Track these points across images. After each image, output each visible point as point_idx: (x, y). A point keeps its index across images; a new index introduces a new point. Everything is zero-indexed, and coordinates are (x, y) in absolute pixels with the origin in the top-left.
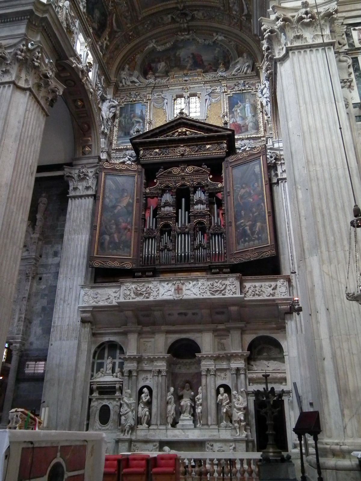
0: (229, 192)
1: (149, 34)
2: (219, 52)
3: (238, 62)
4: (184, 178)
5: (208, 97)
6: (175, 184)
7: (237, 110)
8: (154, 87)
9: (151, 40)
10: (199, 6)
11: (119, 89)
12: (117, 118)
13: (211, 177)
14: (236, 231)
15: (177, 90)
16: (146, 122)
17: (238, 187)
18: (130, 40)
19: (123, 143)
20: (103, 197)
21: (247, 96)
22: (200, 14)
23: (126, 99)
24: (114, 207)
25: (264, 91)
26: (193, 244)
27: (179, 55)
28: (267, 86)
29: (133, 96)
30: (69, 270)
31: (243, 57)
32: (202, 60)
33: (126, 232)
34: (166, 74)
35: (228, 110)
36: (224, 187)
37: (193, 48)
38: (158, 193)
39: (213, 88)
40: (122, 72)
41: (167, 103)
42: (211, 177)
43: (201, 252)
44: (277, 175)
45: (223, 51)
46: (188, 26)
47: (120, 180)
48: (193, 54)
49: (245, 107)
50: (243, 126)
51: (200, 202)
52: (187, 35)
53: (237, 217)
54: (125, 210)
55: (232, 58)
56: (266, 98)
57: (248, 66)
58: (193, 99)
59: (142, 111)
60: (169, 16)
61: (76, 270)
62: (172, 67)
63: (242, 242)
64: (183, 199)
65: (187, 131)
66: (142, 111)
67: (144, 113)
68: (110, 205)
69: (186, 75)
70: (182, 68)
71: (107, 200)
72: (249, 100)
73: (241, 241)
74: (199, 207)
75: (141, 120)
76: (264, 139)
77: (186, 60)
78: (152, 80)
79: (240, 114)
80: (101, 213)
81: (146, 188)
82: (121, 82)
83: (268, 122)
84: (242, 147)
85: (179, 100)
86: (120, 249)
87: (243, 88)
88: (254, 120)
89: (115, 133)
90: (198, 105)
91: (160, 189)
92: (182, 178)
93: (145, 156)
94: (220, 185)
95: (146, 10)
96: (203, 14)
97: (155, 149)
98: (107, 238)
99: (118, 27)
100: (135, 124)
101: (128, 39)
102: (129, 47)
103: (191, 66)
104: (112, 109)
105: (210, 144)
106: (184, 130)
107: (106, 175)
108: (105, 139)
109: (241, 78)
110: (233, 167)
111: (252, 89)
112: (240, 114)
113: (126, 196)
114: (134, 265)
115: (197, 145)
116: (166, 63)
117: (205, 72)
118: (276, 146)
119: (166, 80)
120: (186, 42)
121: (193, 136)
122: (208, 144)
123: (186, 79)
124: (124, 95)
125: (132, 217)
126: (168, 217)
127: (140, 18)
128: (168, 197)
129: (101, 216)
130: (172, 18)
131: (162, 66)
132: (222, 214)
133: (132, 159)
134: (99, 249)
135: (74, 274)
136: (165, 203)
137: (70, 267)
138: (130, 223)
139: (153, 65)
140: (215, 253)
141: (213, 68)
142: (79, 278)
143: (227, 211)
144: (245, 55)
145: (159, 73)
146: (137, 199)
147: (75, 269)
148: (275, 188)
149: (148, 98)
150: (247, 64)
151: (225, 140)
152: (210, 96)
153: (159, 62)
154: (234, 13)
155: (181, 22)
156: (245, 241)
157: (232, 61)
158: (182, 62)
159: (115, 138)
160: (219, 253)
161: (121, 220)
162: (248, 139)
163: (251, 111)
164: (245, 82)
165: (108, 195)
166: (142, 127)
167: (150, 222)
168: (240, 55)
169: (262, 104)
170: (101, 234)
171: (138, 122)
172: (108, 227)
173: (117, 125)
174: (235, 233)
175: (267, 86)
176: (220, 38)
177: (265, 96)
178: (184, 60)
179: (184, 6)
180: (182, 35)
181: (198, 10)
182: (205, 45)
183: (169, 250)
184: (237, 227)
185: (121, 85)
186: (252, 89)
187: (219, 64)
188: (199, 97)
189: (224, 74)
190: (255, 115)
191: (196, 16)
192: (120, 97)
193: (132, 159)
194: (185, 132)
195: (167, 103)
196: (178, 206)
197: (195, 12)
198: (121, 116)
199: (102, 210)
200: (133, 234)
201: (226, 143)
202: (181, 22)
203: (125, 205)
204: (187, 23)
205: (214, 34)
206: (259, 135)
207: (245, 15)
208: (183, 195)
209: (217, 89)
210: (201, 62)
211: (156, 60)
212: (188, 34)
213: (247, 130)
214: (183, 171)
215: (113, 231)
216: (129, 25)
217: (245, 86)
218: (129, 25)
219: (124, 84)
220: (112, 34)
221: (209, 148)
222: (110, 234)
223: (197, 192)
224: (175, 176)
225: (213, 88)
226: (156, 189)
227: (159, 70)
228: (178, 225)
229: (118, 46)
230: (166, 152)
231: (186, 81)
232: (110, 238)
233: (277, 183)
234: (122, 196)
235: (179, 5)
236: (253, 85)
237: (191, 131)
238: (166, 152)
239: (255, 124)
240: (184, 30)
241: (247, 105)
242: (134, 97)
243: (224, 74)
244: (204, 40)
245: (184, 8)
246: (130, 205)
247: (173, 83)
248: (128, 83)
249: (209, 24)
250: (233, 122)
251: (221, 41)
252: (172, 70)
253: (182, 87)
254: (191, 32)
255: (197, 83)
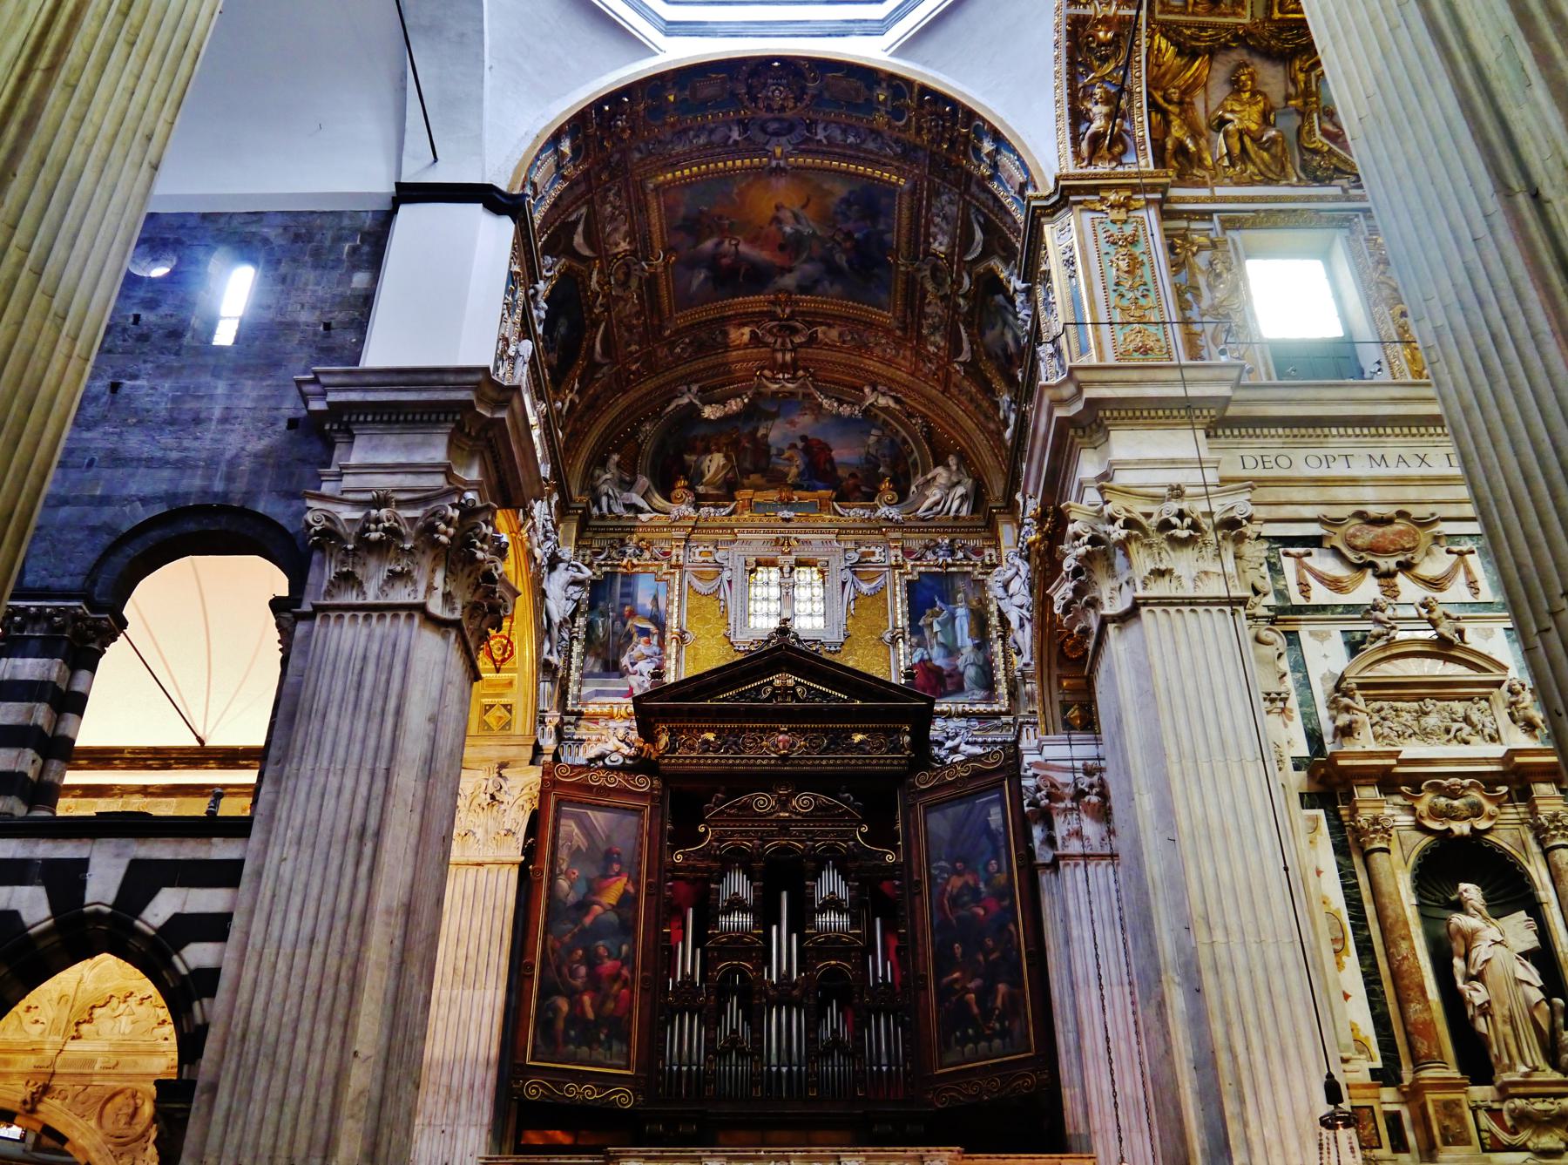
0: (920, 882)
1: (682, 370)
2: (879, 441)
3: (934, 478)
4: (787, 829)
5: (848, 574)
6: (762, 846)
7: (931, 625)
8: (694, 528)
9: (688, 385)
10: (835, 317)
11: (592, 523)
12: (582, 615)
13: (865, 829)
14: (939, 1003)
15: (757, 544)
16: (668, 636)
17: (942, 869)
18: (628, 381)
19: (598, 693)
20: (552, 870)
21: (960, 584)
22: (834, 333)
23: (609, 557)
24: (583, 906)
25: (1015, 586)
26: (816, 1040)
27: (766, 436)
28: (1023, 573)
29: (630, 551)
30: (441, 1101)
31: (947, 466)
32: (831, 460)
33: (616, 987)
34: (727, 490)
35: (907, 623)
36: (902, 865)
37: (805, 422)
38: (708, 869)
39: (863, 549)
40: (597, 472)
41: (730, 582)
42: (865, 829)
43: (835, 1067)
44: (1050, 841)
45: (892, 441)
46: (794, 360)
47: (598, 818)
48: (804, 438)
49: (953, 617)
50: (950, 675)
51: (833, 904)
52: (787, 380)
53: (944, 961)
54: (612, 917)
55: (915, 464)
56: (1021, 607)
57: (963, 498)
58: (804, 575)
59: (655, 599)
60: (747, 330)
61: (464, 1102)
62: (746, 473)
63: (958, 1041)
64: (784, 895)
65: (798, 683)
66: (655, 599)
67: (662, 606)
68: (572, 898)
69: (787, 504)
70: (776, 479)
71: (563, 883)
72: (966, 595)
73: (953, 1039)
74: (830, 920)
75: (652, 627)
76: (1010, 719)
77: (787, 454)
78: (687, 510)
79: (940, 638)
80: (546, 924)
81: (673, 850)
82: (597, 503)
83: (1023, 675)
84: (948, 738)
85: (762, 574)
86: (600, 1043)
87: (949, 560)
88: (981, 656)
89: (575, 662)
90: (819, 592)
91: (715, 858)
92: (781, 828)
93: (675, 750)
94: (890, 858)
95: (688, 312)
96: (841, 335)
97: (702, 731)
98: (563, 1005)
99: (604, 353)
100: (635, 639)
101: (622, 383)
102: (623, 402)
103: (800, 474)
104: (572, 589)
105: (863, 731)
106: (790, 682)
107: (559, 803)
108: (552, 682)
109: (942, 529)
110: (928, 809)
111: (975, 565)
112: (940, 638)
113: (618, 874)
114: (640, 1098)
115: (826, 732)
116: (727, 457)
117: (843, 497)
118: (1049, 752)
119: (728, 510)
120: (785, 403)
121: (818, 702)
122: (858, 731)
123: (786, 514)
124: (604, 544)
125: (635, 941)
126: (737, 945)
127: (668, 333)
128: (738, 884)
129: (545, 933)
130: (752, 332)
131: (714, 464)
132: (898, 950)
133: (626, 750)
134: (539, 1042)
135: (457, 1116)
136: (730, 902)
137: (443, 1092)
138: (628, 960)
139: (690, 458)
140: (880, 1069)
141: (864, 489)
142: (473, 1130)
143: (914, 939)
144: (952, 460)
145: (706, 485)
146: (649, 885)
147: (458, 1101)
148: (1045, 878)
149: (674, 561)
150: (960, 490)
151: (906, 723)
152: (855, 573)
153: (708, 451)
154: (932, 349)
155: (778, 346)
156: (965, 1039)
157: (916, 474)
158: (774, 459)
159: (575, 675)
160: (889, 1069)
161: (601, 950)
162: (964, 715)
163: (970, 630)
164: (952, 541)
165: (564, 867)
166: (657, 649)
167: (688, 960)
168: (940, 461)
169: (1004, 621)
170: (544, 994)
171: (644, 632)
172: (565, 970)
173: (582, 636)
174: (938, 1012)
175: (1023, 573)
176: (882, 401)
177: (1017, 600)
178: (780, 452)
179: (792, 312)
180: (774, 380)
181: (829, 326)
182: (839, 415)
183: (742, 1054)
184: (944, 993)
185: (595, 511)
186: (975, 565)
187: (881, 480)
188: (822, 572)
189: (894, 513)
190: (982, 644)
191: (820, 335)
192: (590, 547)
193: (626, 750)
194: (793, 688)
195: (730, 582)
196: (766, 914)
197: (820, 329)
198: (592, 606)
199: (547, 915)
200: (637, 997)
201: (908, 733)
202: (778, 346)
203: (614, 902)
204: (794, 350)
205: (867, 390)
206: (996, 708)
207: (963, 364)
208: (784, 878)
209: (873, 554)
210: (828, 467)
211: (700, 445)
212: (794, 379)
213: (960, 689)
214: (784, 804)
215: (578, 983)
216: (634, 348)
217: (952, 553)
218: (634, 348)
219: (605, 509)
220: (586, 380)
221: (861, 742)
222: (573, 995)
223: (825, 874)
224: (761, 818)
225: (863, 549)
226: (705, 854)
227: (708, 476)
228: (770, 975)
229: (598, 398)
230: (735, 743)
231: (785, 520)
232: (571, 1006)
233: (1054, 866)
234: (606, 876)
235: (779, 310)
236: (978, 552)
237: (808, 687)
238: (735, 743)
239: (984, 672)
240: (784, 367)
241: (961, 612)
242: (636, 556)
243: (894, 513)
244: (838, 400)
245: (792, 317)
246: (627, 901)
247: (750, 523)
248: (618, 509)
249: (854, 360)
250: (922, 660)
251: (886, 409)
252: (746, 481)
253: (774, 536)
254: (801, 373)
255: (821, 530)
